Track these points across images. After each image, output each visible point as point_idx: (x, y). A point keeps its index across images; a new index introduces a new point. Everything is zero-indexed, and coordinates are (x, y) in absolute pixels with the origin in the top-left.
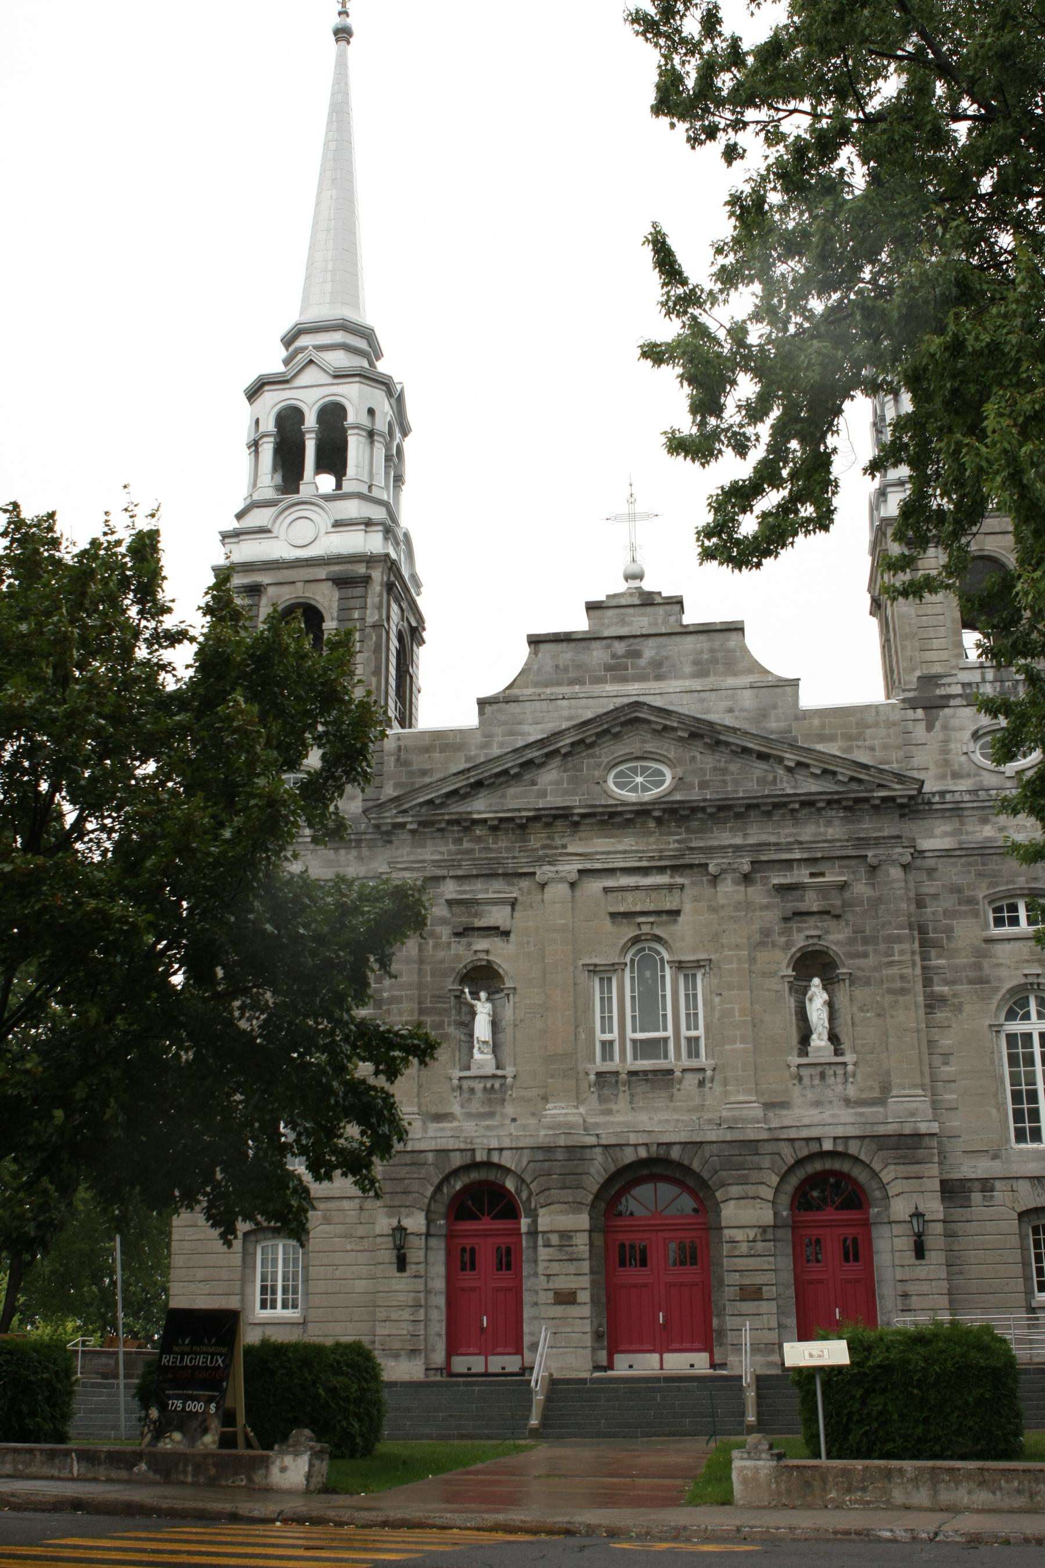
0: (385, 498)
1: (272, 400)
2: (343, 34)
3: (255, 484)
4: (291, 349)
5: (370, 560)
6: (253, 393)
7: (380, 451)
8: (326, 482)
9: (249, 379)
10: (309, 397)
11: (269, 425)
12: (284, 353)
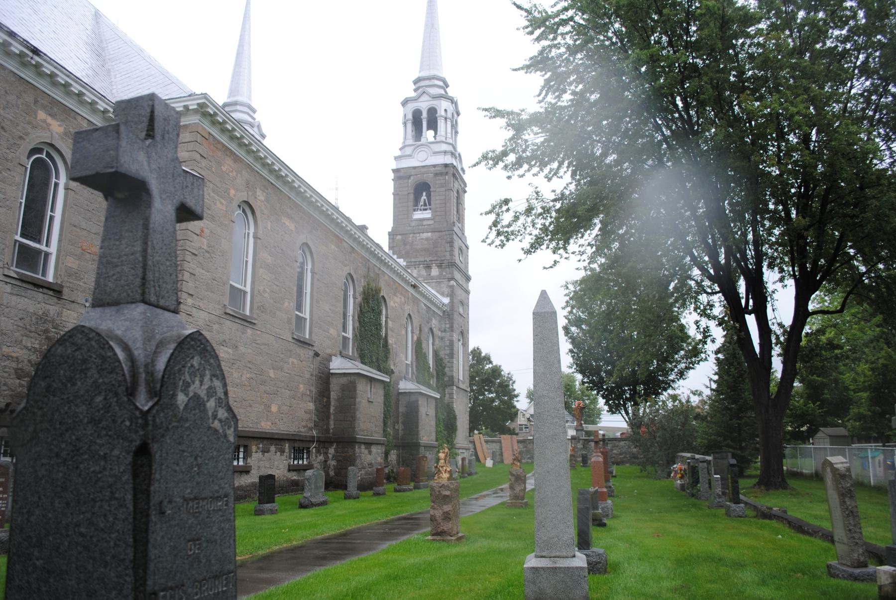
1: (412, 106)
3: (405, 138)
5: (446, 166)
6: (405, 103)
7: (449, 124)
8: (429, 135)
10: (424, 105)
11: (410, 116)
12: (414, 87)
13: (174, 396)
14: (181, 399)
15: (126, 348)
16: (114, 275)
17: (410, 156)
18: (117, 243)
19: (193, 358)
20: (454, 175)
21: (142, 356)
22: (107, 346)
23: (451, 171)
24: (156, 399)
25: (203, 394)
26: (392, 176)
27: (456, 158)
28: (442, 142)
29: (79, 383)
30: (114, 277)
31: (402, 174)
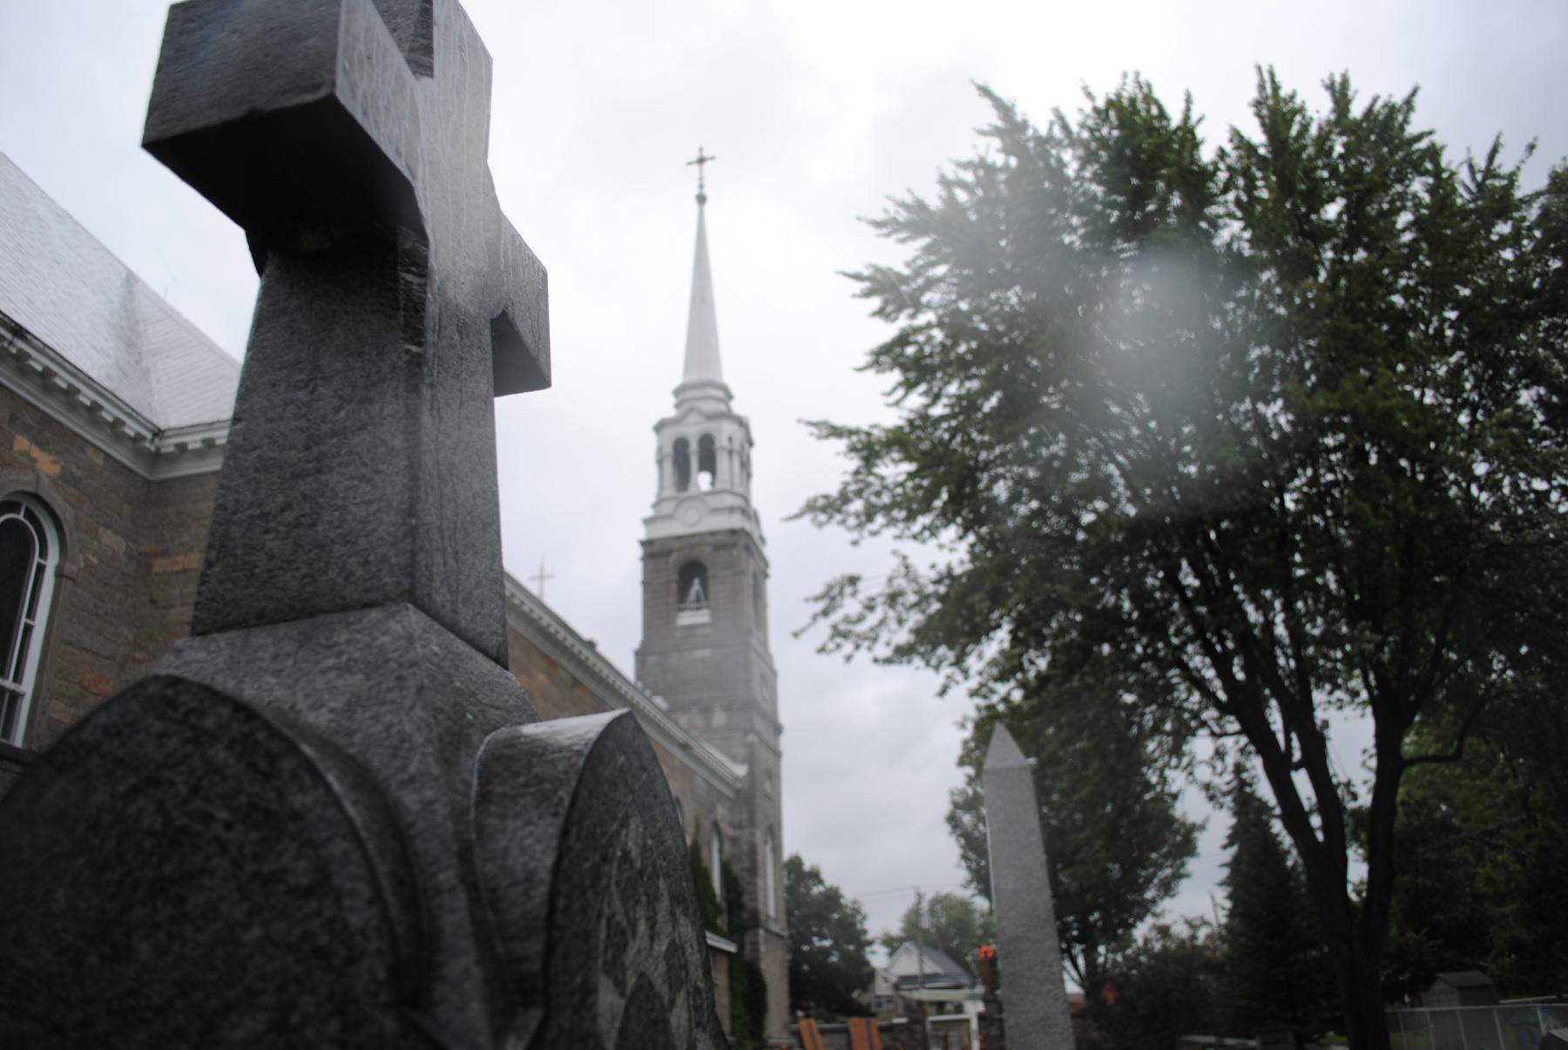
1: (671, 433)
2: (701, 199)
5: (733, 532)
6: (659, 428)
8: (703, 480)
9: (655, 420)
10: (692, 431)
11: (669, 450)
12: (672, 400)
16: (287, 507)
18: (302, 395)
22: (286, 764)
23: (743, 540)
26: (638, 552)
29: (144, 950)
30: (289, 516)
31: (656, 548)
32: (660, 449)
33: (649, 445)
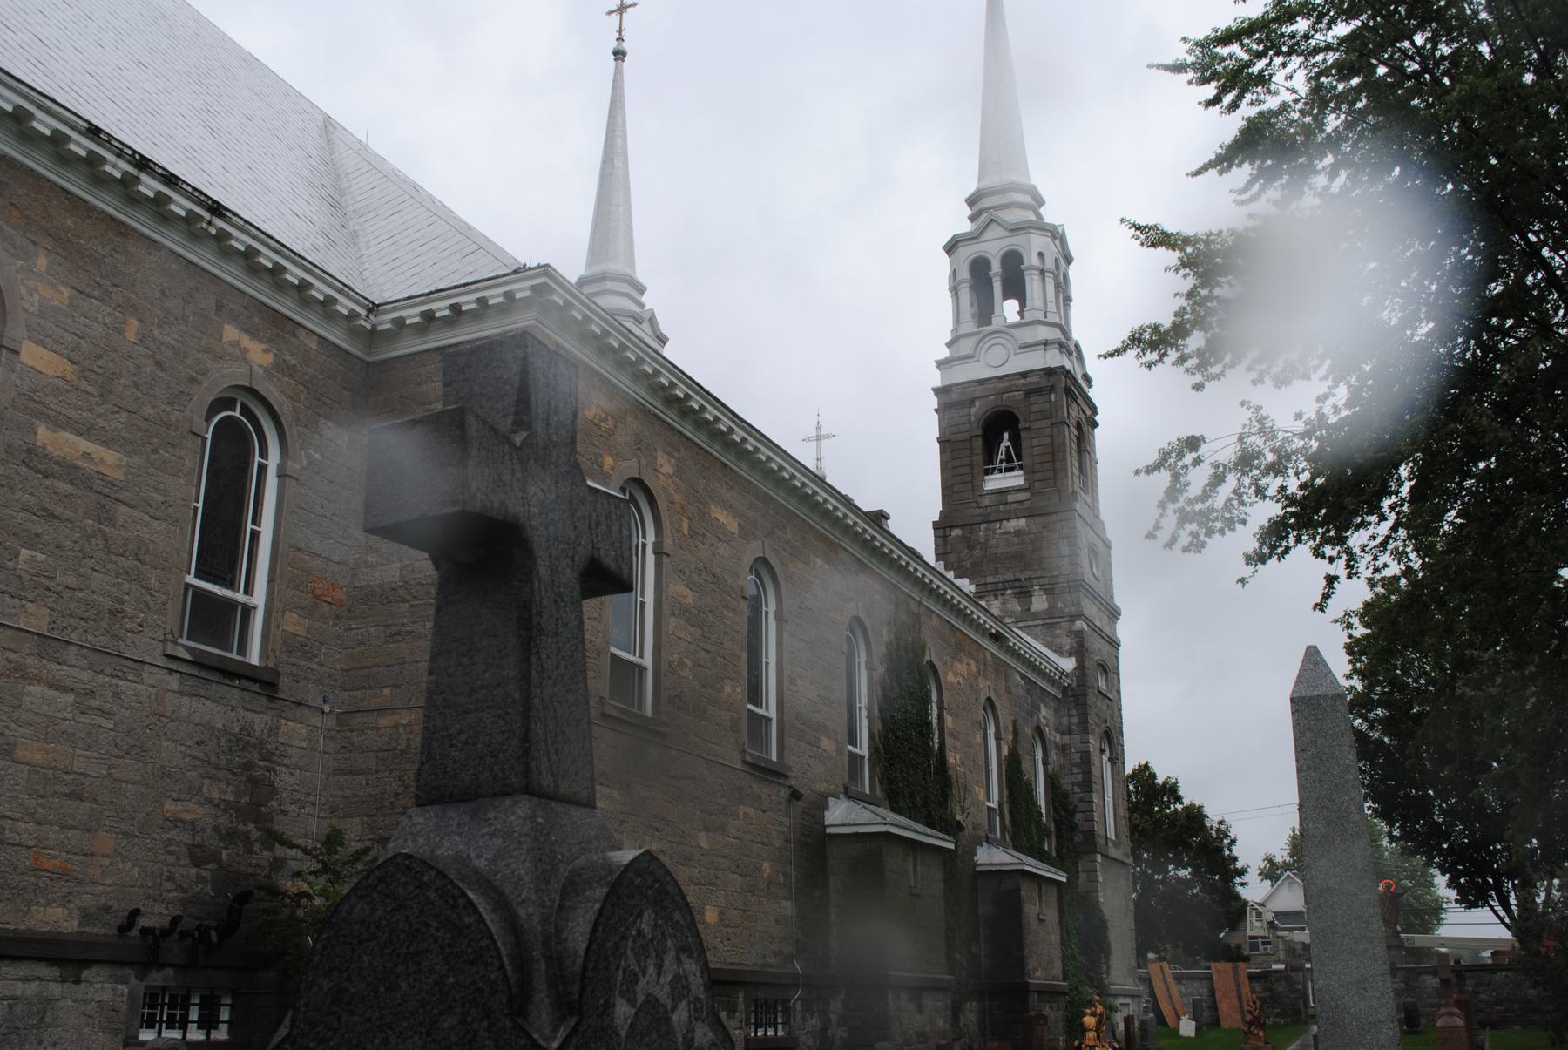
0: (1057, 320)
1: (967, 253)
4: (978, 207)
5: (1049, 372)
6: (951, 247)
9: (945, 239)
10: (993, 248)
11: (965, 274)
12: (969, 212)
13: (609, 1006)
14: (623, 1011)
15: (503, 905)
16: (461, 731)
17: (969, 357)
18: (465, 661)
19: (640, 915)
20: (1068, 391)
21: (536, 919)
22: (461, 901)
24: (572, 1021)
25: (663, 995)
26: (934, 402)
27: (1070, 354)
28: (1039, 322)
29: (404, 985)
30: (463, 737)
31: (955, 397)
32: (954, 273)
33: (942, 265)
